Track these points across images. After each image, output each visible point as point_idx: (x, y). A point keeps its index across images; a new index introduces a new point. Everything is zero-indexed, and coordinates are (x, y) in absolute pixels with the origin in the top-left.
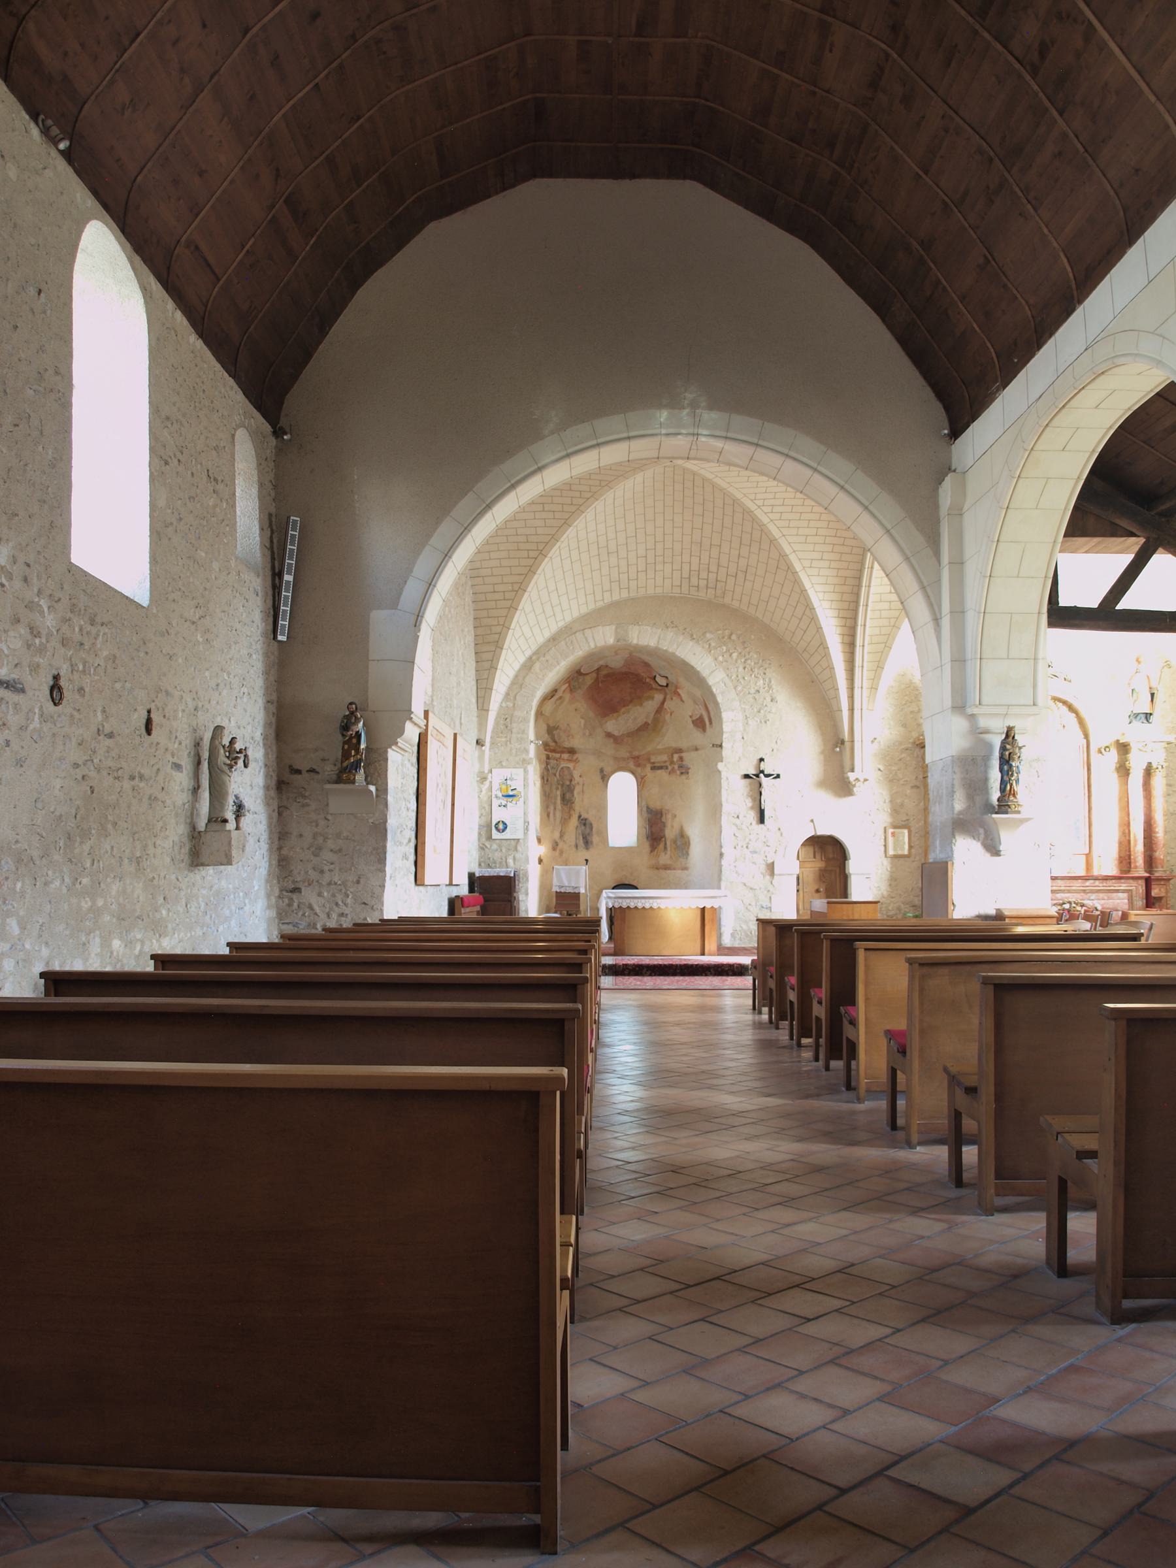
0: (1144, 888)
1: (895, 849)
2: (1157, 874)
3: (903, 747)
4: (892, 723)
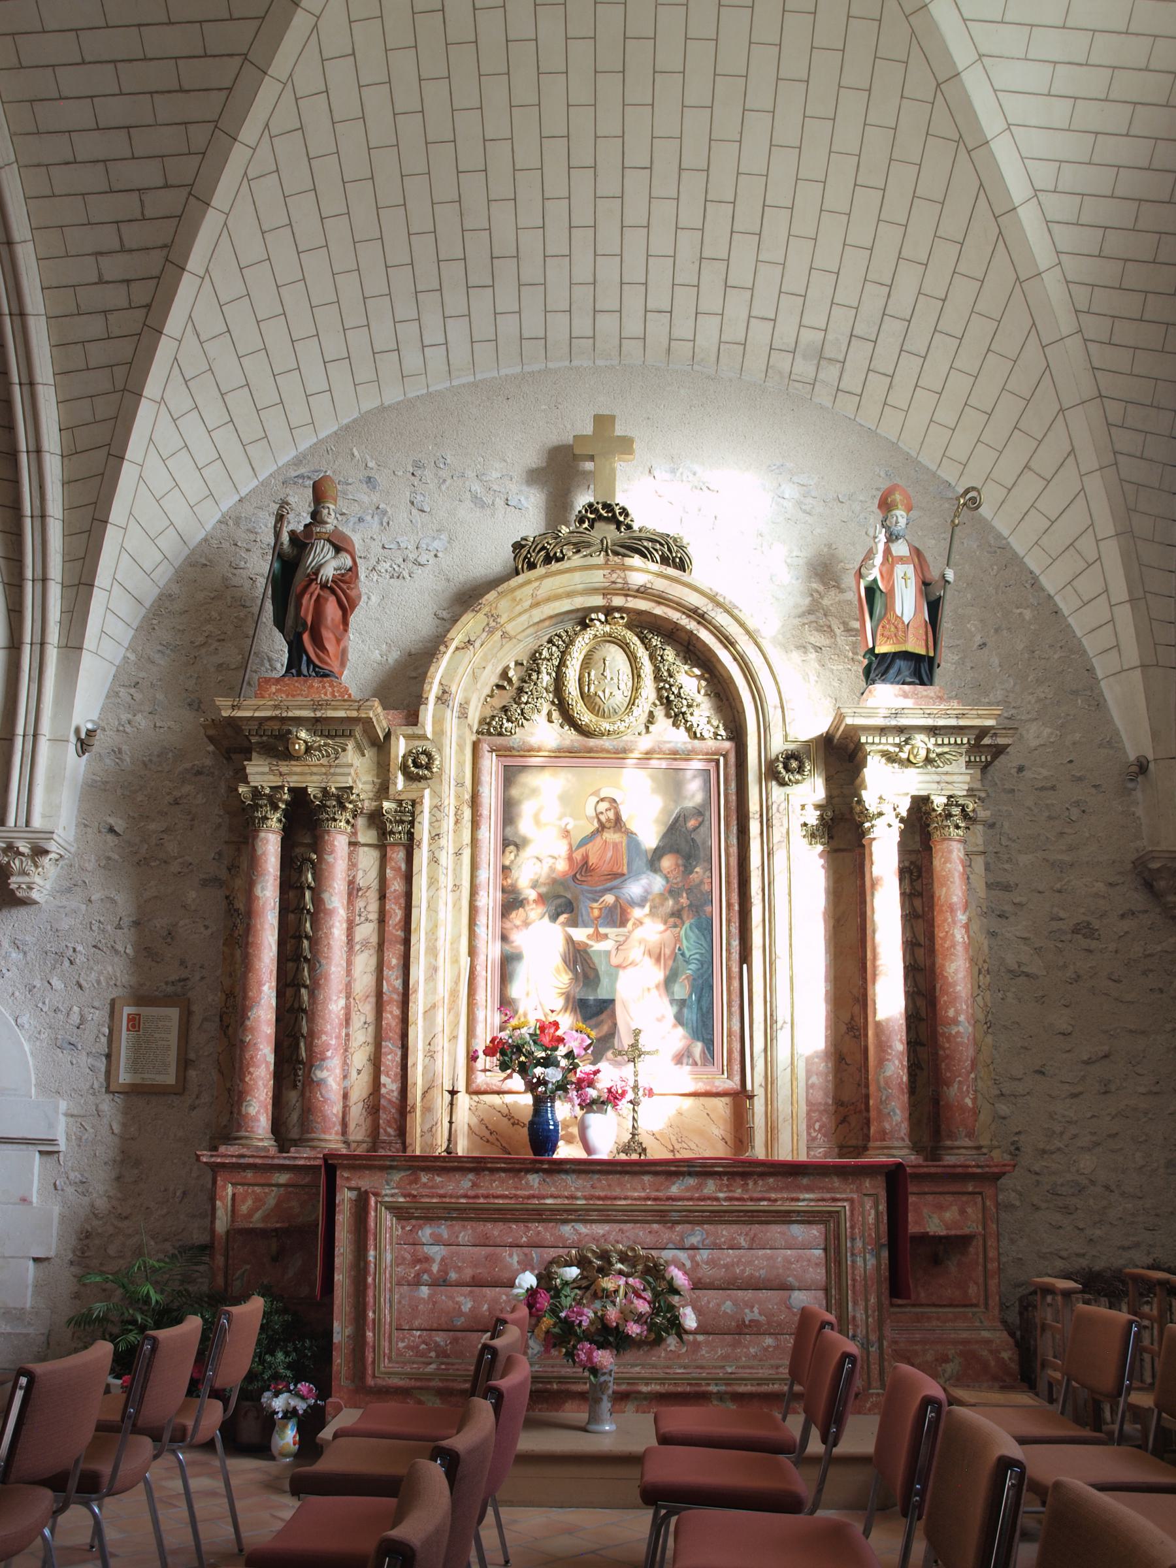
0: (882, 1207)
1: (136, 1066)
2: (950, 1160)
3: (188, 765)
4: (160, 696)
